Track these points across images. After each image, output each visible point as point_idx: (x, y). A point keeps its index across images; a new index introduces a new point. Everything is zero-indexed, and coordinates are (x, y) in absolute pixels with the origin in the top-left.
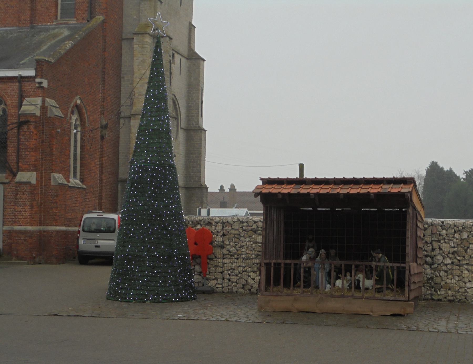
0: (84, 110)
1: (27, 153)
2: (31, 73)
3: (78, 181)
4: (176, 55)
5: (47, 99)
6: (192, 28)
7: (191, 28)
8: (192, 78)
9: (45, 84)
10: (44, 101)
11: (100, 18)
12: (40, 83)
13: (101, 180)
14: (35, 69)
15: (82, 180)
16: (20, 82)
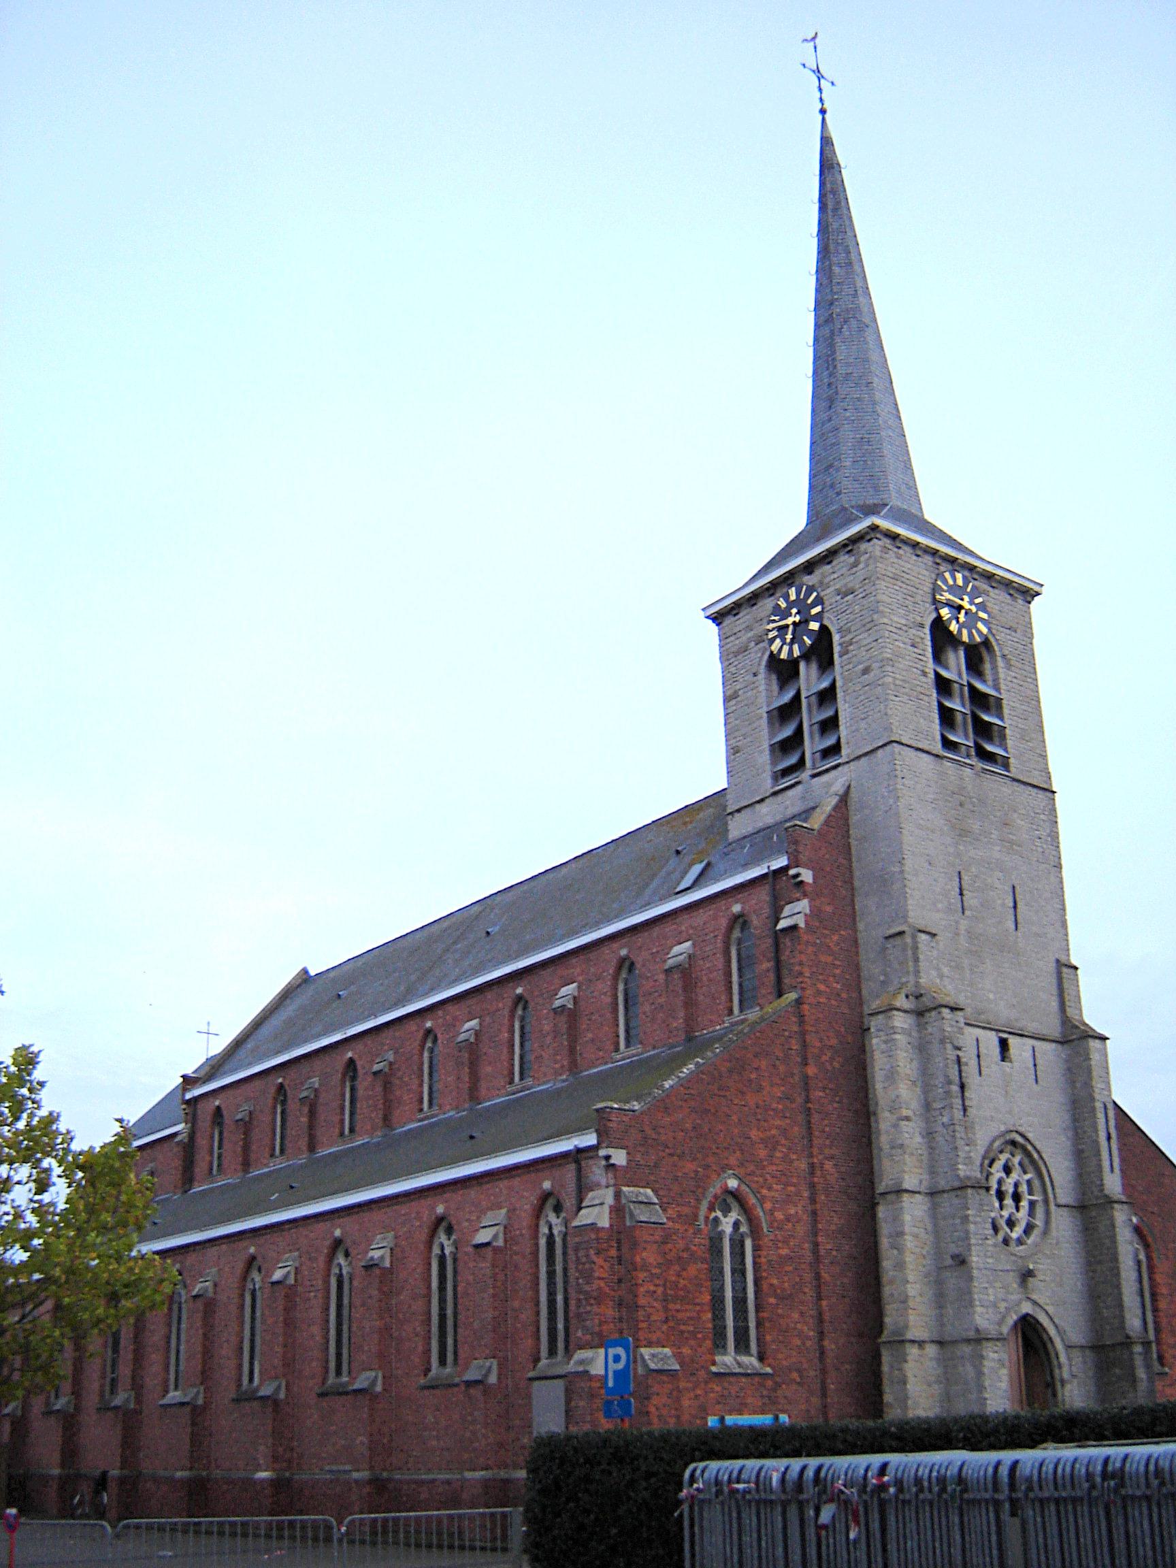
0: (753, 1200)
1: (589, 1308)
2: (590, 1139)
3: (754, 1361)
4: (1013, 1041)
5: (625, 1189)
6: (1065, 970)
7: (1065, 970)
8: (1078, 1085)
9: (620, 1157)
10: (618, 1195)
11: (793, 996)
12: (608, 1158)
13: (822, 1352)
14: (596, 1131)
15: (761, 1358)
16: (577, 1162)
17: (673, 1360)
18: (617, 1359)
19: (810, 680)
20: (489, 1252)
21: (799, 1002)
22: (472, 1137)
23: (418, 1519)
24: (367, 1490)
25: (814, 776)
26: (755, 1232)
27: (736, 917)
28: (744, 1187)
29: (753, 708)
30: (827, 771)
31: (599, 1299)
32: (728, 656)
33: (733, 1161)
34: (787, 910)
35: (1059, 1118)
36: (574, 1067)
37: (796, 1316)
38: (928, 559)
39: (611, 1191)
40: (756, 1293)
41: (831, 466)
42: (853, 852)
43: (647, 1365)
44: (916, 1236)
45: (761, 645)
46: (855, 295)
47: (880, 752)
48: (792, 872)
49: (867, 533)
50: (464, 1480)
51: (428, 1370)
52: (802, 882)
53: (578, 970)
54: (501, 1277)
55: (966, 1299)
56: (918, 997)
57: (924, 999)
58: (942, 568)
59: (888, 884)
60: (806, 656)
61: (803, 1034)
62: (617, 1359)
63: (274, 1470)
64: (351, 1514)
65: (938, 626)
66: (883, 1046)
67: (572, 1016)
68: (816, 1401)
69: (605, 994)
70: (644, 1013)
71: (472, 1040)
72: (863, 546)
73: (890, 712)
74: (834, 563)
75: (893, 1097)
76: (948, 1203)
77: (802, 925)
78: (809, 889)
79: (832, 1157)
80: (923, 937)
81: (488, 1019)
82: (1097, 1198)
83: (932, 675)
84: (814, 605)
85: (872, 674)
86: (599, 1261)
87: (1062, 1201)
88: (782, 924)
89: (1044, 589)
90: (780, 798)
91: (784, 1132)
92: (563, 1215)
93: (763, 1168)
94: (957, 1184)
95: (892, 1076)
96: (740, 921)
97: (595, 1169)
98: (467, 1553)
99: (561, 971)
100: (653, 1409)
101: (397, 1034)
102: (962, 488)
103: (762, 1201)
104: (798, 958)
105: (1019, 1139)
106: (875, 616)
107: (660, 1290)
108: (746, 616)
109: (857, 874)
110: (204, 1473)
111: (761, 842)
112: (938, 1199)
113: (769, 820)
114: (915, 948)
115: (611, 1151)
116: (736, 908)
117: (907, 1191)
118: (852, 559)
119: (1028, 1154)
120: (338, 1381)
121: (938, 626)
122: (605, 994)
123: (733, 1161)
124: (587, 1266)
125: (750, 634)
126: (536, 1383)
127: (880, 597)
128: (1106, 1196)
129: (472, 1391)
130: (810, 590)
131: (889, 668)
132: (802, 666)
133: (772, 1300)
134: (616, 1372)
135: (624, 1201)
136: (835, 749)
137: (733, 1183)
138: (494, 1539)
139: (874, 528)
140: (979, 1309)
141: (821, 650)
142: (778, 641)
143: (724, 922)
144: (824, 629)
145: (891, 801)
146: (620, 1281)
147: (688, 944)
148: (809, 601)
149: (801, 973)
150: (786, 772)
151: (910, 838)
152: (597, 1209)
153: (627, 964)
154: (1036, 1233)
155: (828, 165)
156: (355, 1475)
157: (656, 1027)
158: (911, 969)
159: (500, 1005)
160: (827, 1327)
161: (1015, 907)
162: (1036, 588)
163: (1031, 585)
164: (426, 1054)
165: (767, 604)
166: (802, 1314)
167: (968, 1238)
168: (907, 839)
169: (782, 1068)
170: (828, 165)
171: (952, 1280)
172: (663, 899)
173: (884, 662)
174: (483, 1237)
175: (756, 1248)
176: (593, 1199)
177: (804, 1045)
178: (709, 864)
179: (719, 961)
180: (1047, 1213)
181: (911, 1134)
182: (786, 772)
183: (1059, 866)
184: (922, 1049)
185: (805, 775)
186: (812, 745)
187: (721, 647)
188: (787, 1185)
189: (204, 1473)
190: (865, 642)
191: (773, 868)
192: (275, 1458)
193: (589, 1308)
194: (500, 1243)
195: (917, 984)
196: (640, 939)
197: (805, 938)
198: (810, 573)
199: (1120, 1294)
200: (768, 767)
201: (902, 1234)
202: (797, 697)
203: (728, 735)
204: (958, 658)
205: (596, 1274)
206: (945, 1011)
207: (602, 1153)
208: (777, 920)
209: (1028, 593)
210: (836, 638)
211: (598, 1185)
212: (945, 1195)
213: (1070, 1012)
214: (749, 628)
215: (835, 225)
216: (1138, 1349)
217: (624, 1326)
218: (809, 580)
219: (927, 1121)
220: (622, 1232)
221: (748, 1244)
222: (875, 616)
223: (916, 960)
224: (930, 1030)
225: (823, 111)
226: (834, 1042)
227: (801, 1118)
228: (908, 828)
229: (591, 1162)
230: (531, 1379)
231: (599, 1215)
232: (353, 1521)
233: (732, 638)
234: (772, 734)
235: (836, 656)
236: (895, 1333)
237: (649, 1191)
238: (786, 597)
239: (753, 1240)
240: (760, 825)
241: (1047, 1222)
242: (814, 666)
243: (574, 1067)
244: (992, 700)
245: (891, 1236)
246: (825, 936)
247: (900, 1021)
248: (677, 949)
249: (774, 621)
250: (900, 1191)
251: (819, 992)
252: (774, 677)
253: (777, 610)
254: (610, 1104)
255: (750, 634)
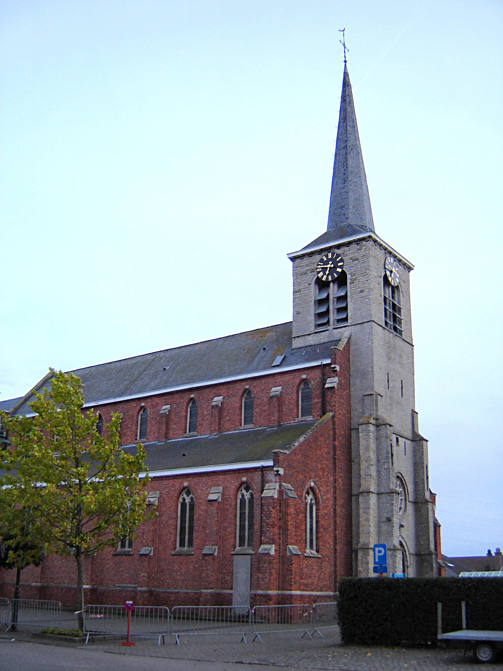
0: (318, 491)
1: (268, 529)
2: (270, 463)
3: (314, 552)
4: (400, 438)
5: (283, 484)
6: (415, 414)
7: (414, 413)
8: (417, 457)
9: (281, 471)
10: (280, 486)
11: (331, 414)
12: (277, 471)
13: (335, 550)
14: (273, 460)
15: (317, 551)
16: (262, 471)
17: (298, 551)
18: (380, 551)
19: (334, 291)
20: (216, 504)
21: (333, 417)
22: (184, 455)
23: (184, 609)
24: (145, 595)
25: (335, 329)
26: (317, 503)
27: (303, 380)
28: (316, 486)
29: (307, 297)
30: (341, 327)
31: (273, 526)
32: (296, 275)
33: (313, 476)
34: (329, 380)
35: (411, 469)
36: (220, 430)
37: (328, 536)
38: (383, 251)
39: (278, 484)
40: (316, 526)
41: (344, 206)
42: (351, 360)
43: (292, 552)
44: (373, 509)
45: (314, 273)
46: (356, 140)
47: (366, 324)
48: (332, 366)
49: (367, 238)
50: (201, 593)
51: (175, 548)
52: (336, 370)
53: (223, 391)
54: (220, 514)
55: (390, 534)
56: (377, 419)
57: (379, 420)
58: (387, 256)
59: (366, 375)
60: (334, 281)
61: (334, 429)
62: (380, 551)
63: (91, 585)
64: (256, 605)
65: (385, 277)
66: (364, 437)
67: (220, 409)
68: (332, 568)
69: (237, 402)
70: (256, 412)
71: (167, 413)
72: (364, 243)
73: (371, 309)
74: (350, 247)
75: (368, 456)
76: (385, 498)
77: (336, 387)
78: (338, 373)
79: (341, 477)
80: (379, 397)
81: (175, 406)
82: (422, 500)
83: (383, 297)
84: (339, 262)
85: (364, 293)
86: (274, 511)
87: (410, 500)
88: (327, 386)
89: (414, 268)
90: (318, 334)
91: (327, 466)
92: (250, 491)
93: (321, 479)
94: (389, 491)
95: (367, 448)
96: (305, 381)
97: (269, 475)
98: (233, 622)
99: (215, 390)
100: (293, 569)
101: (125, 406)
102: (388, 223)
103: (320, 491)
104: (335, 400)
105: (400, 476)
106: (368, 271)
107: (294, 524)
108: (306, 260)
109: (352, 369)
110: (46, 584)
111: (312, 352)
112: (381, 496)
113: (312, 343)
114: (377, 402)
115: (280, 469)
116: (304, 376)
117: (372, 492)
118: (358, 247)
119: (402, 481)
120: (123, 549)
121: (385, 277)
122: (237, 402)
123: (313, 476)
124: (268, 512)
125: (308, 268)
126: (236, 556)
127: (370, 264)
128: (426, 499)
129: (207, 558)
130: (338, 256)
131: (372, 292)
132: (331, 284)
133: (322, 530)
134: (379, 557)
135: (283, 488)
136: (346, 319)
137: (313, 484)
138: (214, 616)
139: (370, 237)
140: (395, 538)
141: (342, 280)
142: (322, 273)
143: (298, 381)
144: (343, 272)
145: (370, 344)
146: (280, 519)
147: (280, 387)
148: (337, 260)
149: (334, 406)
150: (319, 325)
151: (376, 358)
152: (272, 491)
153: (247, 391)
154: (402, 511)
155: (346, 84)
156: (139, 589)
157: (261, 418)
158: (375, 409)
159: (182, 401)
160: (338, 542)
161: (402, 388)
162: (412, 267)
163: (411, 266)
164: (140, 417)
165: (318, 257)
166: (330, 536)
167: (392, 512)
168: (375, 359)
169: (328, 441)
170: (346, 84)
171: (385, 527)
172: (265, 369)
173: (370, 290)
174: (212, 497)
175: (317, 510)
176: (270, 486)
177: (335, 433)
178: (285, 357)
179: (295, 397)
180: (406, 504)
181: (373, 471)
182: (319, 325)
183: (413, 374)
184: (378, 439)
185: (331, 327)
186: (333, 316)
187: (293, 271)
188: (327, 486)
189: (46, 584)
190: (362, 280)
191: (323, 363)
192: (92, 580)
193: (268, 529)
194: (220, 500)
195: (377, 415)
196: (255, 383)
197: (336, 392)
198: (338, 249)
199: (429, 536)
200: (313, 322)
201: (369, 508)
202: (328, 296)
203: (294, 307)
204: (389, 290)
205: (273, 516)
206: (388, 426)
207: (275, 469)
208: (324, 384)
209: (409, 268)
210: (349, 276)
211: (271, 481)
212: (384, 495)
213: (416, 430)
214: (307, 265)
215: (349, 110)
216: (434, 556)
217: (281, 536)
218: (337, 251)
219: (378, 466)
220: (282, 500)
221: (314, 508)
222: (368, 271)
223: (377, 405)
224: (381, 432)
225: (345, 62)
226: (343, 433)
227: (332, 461)
228: (375, 355)
229: (268, 472)
230: (232, 555)
231: (274, 493)
232: (176, 609)
233: (299, 268)
234: (315, 310)
235: (348, 283)
236: (363, 545)
237: (290, 485)
238: (327, 256)
239: (316, 506)
240: (308, 344)
241: (406, 507)
242: (336, 285)
243: (220, 430)
244: (397, 307)
245: (364, 509)
246: (342, 392)
247: (372, 428)
248: (273, 389)
249: (321, 265)
250: (369, 492)
251: (340, 413)
252: (317, 287)
253: (322, 260)
254: (280, 450)
255: (308, 268)
